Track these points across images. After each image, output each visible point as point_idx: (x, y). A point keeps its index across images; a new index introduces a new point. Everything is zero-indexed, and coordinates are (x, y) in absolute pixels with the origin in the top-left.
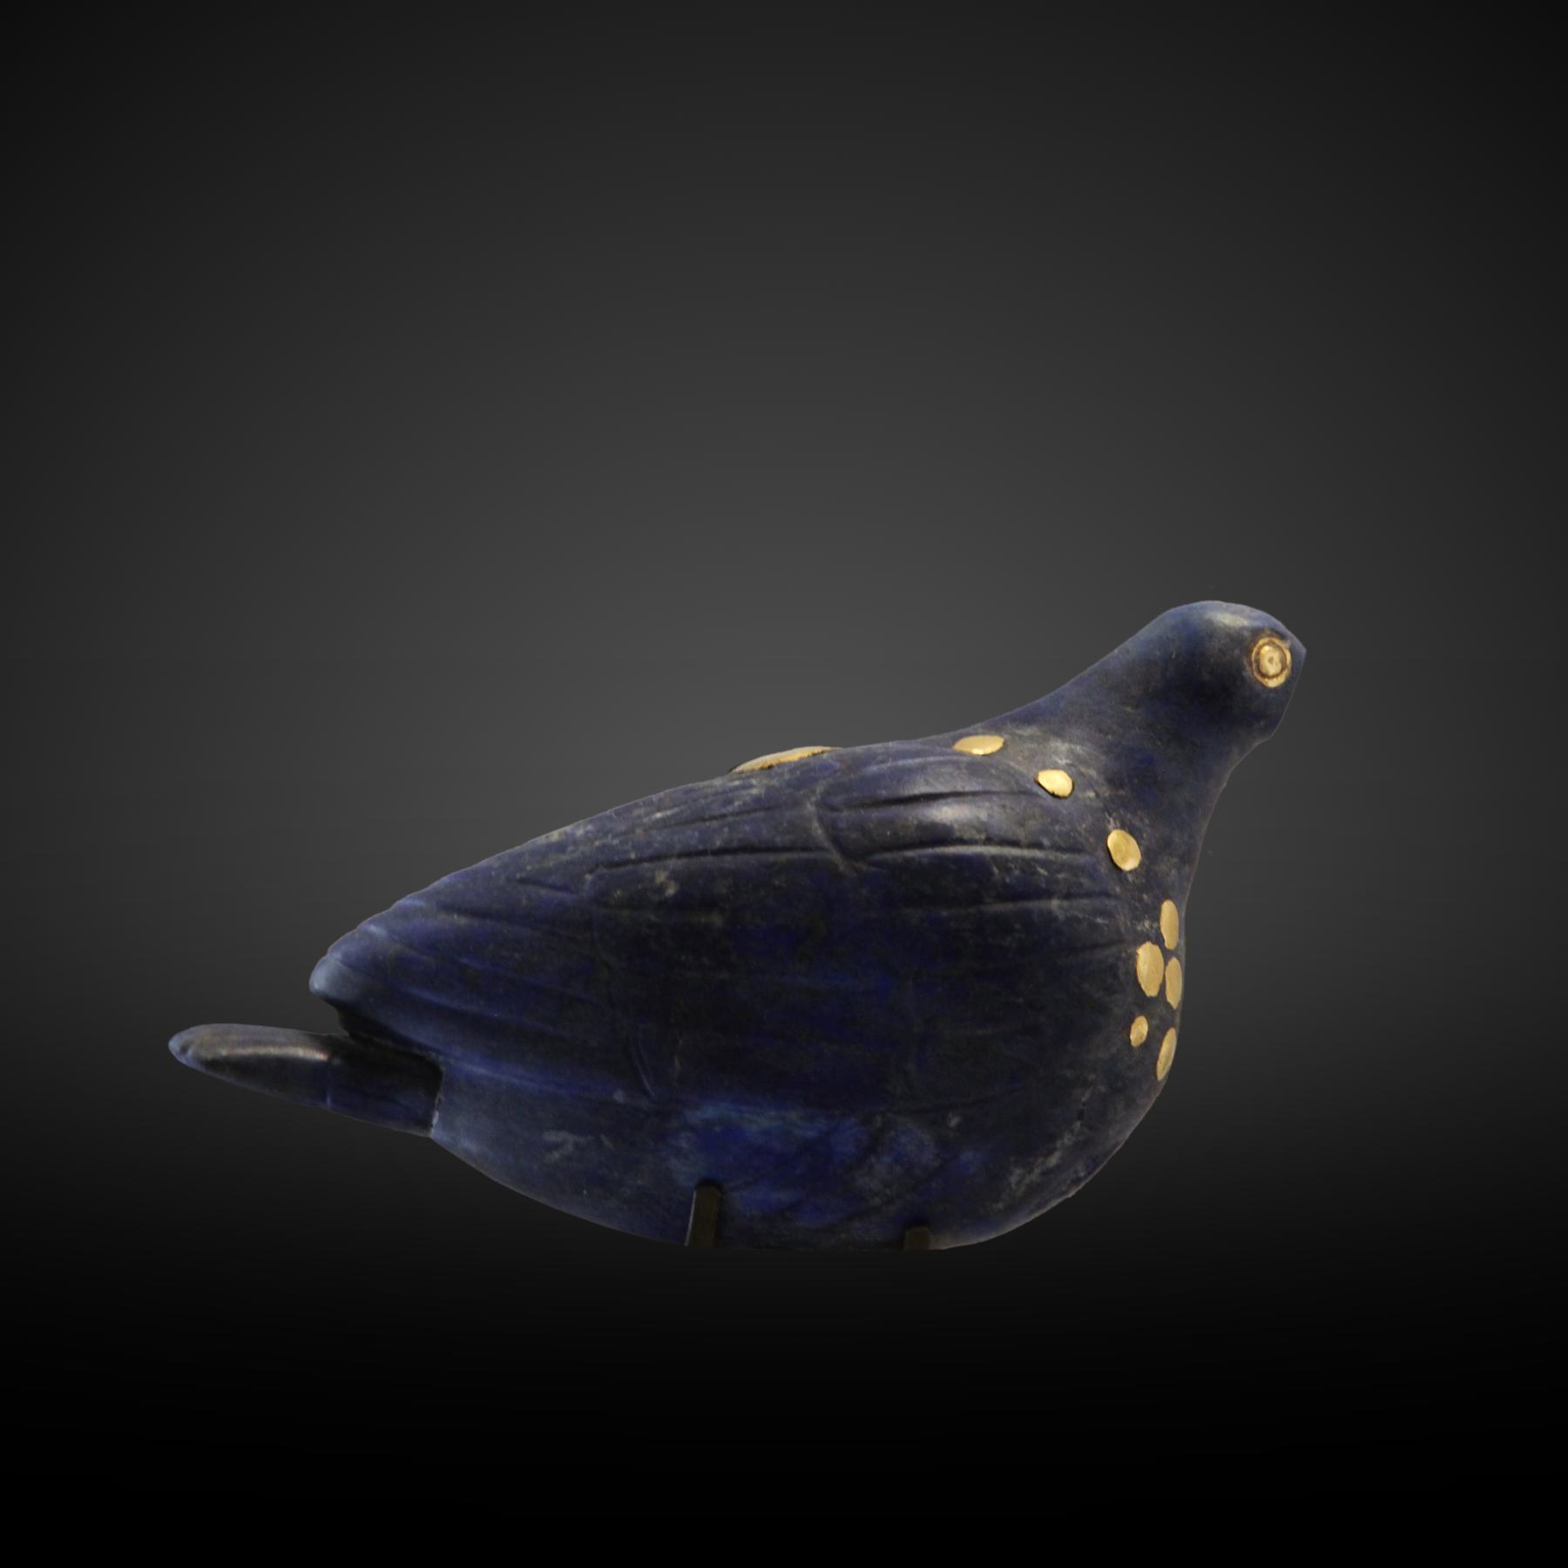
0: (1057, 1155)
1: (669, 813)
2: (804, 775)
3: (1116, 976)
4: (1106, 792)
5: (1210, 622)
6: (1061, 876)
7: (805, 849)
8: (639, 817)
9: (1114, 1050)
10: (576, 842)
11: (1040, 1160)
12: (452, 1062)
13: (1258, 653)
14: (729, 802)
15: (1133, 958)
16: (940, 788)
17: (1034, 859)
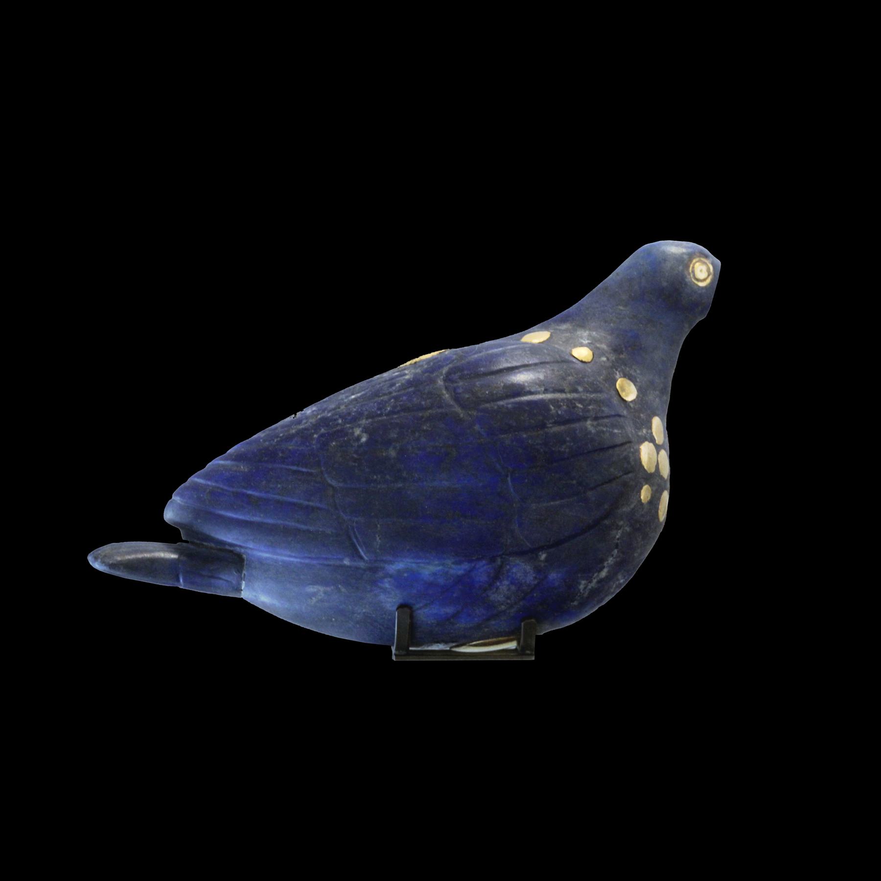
0: (606, 570)
1: (359, 395)
2: (435, 366)
3: (629, 463)
4: (613, 357)
5: (664, 252)
6: (590, 407)
7: (440, 407)
8: (342, 399)
9: (632, 506)
10: (307, 418)
11: (596, 575)
12: (249, 552)
13: (693, 268)
14: (393, 385)
15: (638, 451)
16: (515, 364)
17: (574, 399)
